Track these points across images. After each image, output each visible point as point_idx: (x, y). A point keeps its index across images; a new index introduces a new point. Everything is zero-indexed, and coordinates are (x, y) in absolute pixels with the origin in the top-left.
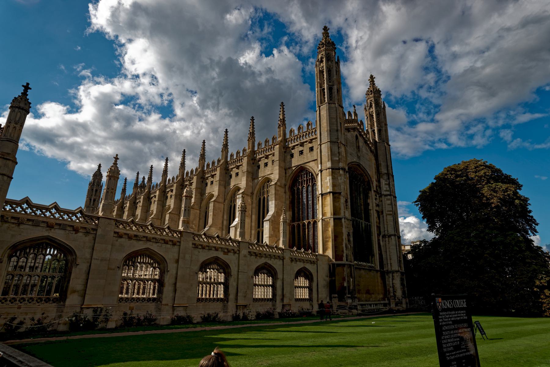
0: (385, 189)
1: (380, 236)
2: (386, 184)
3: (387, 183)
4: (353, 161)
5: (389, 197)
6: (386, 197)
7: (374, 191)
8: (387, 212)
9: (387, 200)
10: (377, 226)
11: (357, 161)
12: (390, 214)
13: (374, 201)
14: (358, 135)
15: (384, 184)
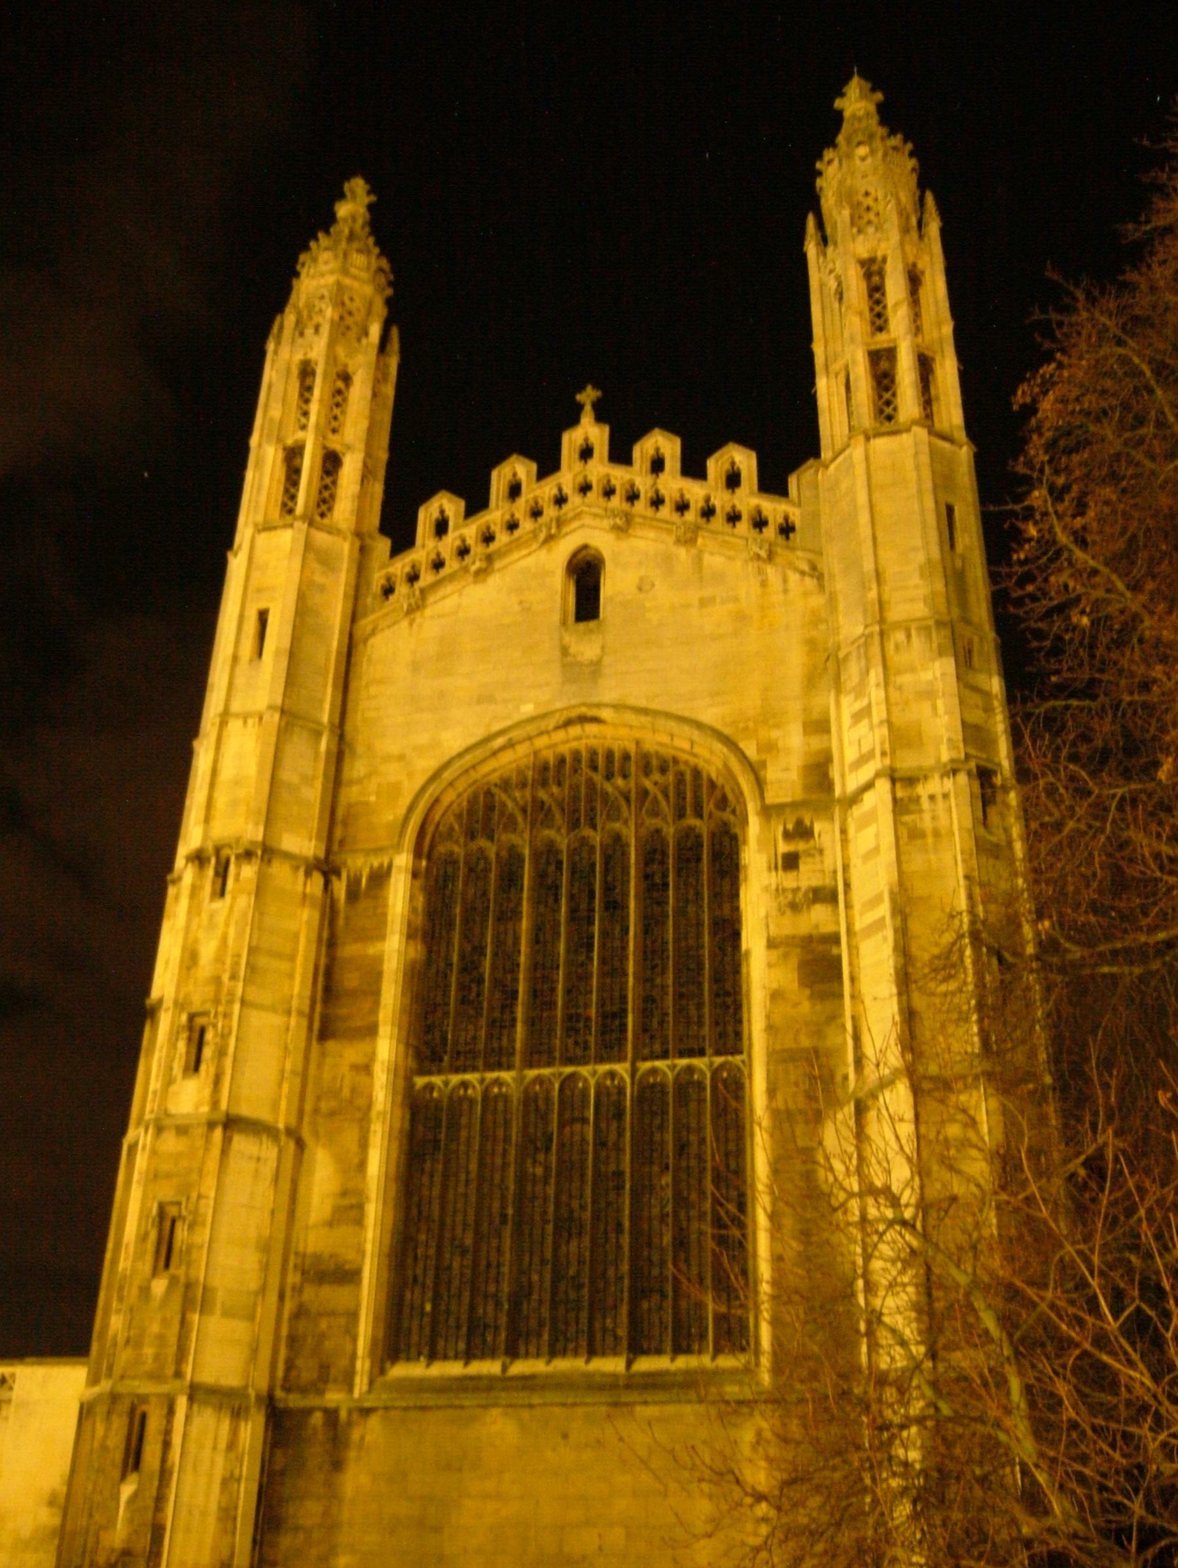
0: (851, 755)
1: (817, 1118)
2: (857, 717)
3: (865, 702)
4: (496, 727)
5: (869, 798)
6: (857, 811)
7: (768, 812)
8: (862, 914)
9: (859, 829)
10: (779, 1058)
11: (558, 705)
12: (879, 925)
13: (773, 879)
14: (602, 541)
15: (846, 720)
